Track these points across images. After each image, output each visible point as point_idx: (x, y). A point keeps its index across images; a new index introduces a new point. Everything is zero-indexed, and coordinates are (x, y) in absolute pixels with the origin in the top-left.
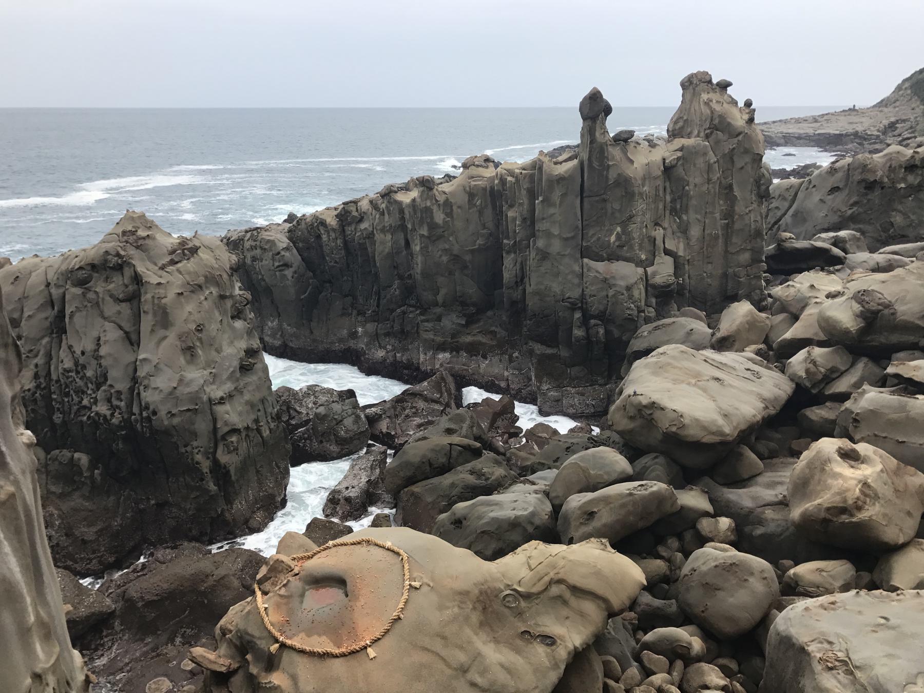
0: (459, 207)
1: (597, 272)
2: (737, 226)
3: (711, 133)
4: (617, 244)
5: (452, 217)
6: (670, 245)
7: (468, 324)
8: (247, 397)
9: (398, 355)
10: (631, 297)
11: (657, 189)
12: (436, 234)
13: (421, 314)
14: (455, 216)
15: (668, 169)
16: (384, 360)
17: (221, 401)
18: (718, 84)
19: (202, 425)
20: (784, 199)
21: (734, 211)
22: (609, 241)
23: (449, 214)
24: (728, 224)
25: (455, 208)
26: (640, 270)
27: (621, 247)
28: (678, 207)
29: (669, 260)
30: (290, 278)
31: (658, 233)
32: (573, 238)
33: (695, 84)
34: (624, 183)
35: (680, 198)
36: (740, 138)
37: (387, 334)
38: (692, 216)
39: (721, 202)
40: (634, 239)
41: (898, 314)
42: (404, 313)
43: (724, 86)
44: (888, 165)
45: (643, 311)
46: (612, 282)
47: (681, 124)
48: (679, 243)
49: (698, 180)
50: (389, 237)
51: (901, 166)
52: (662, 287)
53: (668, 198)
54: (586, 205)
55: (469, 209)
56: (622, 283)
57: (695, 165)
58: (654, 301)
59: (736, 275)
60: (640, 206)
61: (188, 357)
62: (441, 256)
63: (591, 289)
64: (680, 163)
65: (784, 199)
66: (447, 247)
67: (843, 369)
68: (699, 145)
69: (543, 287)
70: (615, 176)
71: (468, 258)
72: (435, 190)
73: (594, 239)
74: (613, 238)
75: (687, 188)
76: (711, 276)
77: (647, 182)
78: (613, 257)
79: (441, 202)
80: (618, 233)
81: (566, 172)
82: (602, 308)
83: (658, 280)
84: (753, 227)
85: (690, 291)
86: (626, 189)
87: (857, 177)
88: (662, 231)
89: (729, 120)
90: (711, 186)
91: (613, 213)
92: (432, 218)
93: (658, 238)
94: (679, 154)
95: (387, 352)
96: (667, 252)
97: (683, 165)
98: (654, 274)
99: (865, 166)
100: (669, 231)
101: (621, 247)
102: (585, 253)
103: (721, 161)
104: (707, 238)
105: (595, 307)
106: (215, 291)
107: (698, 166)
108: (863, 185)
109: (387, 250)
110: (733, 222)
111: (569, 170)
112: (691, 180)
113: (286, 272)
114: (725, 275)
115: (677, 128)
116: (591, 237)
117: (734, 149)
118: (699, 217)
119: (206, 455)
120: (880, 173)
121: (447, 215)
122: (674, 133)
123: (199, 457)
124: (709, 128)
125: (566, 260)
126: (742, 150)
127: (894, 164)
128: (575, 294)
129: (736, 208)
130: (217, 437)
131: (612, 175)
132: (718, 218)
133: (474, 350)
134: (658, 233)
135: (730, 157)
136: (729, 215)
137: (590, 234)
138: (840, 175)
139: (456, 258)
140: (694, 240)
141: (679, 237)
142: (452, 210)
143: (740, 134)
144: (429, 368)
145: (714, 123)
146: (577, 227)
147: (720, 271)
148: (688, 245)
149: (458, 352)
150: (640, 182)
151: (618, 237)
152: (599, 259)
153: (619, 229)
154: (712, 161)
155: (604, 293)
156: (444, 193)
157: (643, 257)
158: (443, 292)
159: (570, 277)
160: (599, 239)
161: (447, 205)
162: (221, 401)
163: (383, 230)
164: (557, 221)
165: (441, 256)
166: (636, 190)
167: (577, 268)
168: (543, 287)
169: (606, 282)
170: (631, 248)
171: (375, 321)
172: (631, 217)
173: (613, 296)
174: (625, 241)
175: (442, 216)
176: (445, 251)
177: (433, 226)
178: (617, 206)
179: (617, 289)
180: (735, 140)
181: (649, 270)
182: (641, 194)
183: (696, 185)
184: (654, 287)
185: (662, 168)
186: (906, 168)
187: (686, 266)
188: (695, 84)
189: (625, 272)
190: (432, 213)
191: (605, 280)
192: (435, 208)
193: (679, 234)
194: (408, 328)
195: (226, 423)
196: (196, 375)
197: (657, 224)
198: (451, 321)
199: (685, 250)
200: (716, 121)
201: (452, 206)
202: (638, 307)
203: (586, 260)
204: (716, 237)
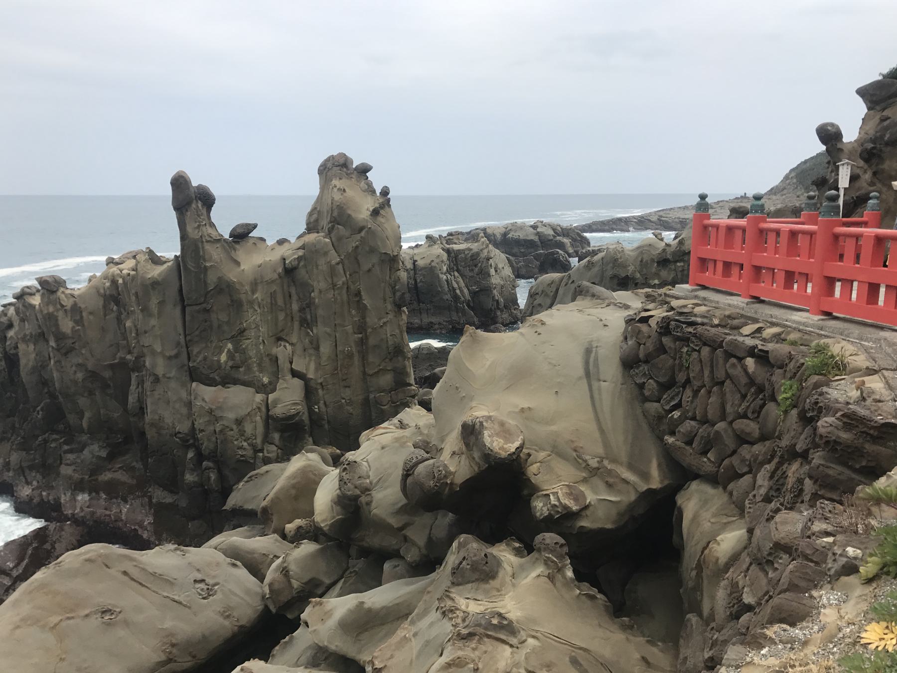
0: (91, 313)
1: (203, 400)
2: (372, 341)
3: (333, 227)
4: (230, 363)
5: (83, 325)
6: (298, 366)
7: (112, 457)
9: (44, 494)
10: (242, 433)
11: (273, 295)
12: (66, 347)
13: (65, 443)
14: (86, 324)
15: (289, 271)
16: (31, 499)
18: (356, 169)
20: (547, 295)
21: (365, 323)
22: (219, 361)
23: (79, 322)
24: (362, 339)
25: (84, 314)
26: (259, 397)
27: (236, 367)
28: (309, 317)
29: (297, 383)
31: (282, 351)
32: (176, 356)
33: (336, 168)
34: (226, 288)
35: (308, 306)
36: (363, 234)
37: (31, 468)
38: (320, 330)
39: (353, 312)
40: (250, 358)
41: (374, 505)
42: (46, 441)
43: (364, 170)
44: (640, 259)
45: (261, 451)
46: (218, 413)
47: (315, 216)
48: (310, 360)
49: (323, 285)
50: (32, 347)
51: (653, 260)
52: (283, 419)
53: (295, 307)
54: (188, 318)
55: (105, 315)
56: (231, 416)
57: (317, 266)
58: (276, 436)
59: (377, 402)
60: (252, 317)
62: (75, 372)
63: (200, 423)
64: (302, 264)
65: (547, 295)
66: (80, 361)
67: (327, 581)
68: (319, 242)
69: (157, 417)
70: (215, 280)
71: (107, 374)
72: (59, 293)
73: (200, 358)
74: (223, 358)
75: (312, 294)
76: (350, 403)
77: (260, 287)
78: (227, 381)
79: (68, 308)
80: (229, 350)
81: (159, 275)
82: (212, 446)
83: (279, 411)
84: (390, 343)
85: (329, 422)
86: (231, 296)
87: (610, 273)
88: (289, 347)
89: (349, 212)
90: (336, 292)
91: (219, 326)
92: (57, 325)
93: (280, 357)
94: (301, 253)
95: (33, 490)
96: (295, 374)
97: (305, 266)
98: (276, 402)
99: (616, 260)
100: (299, 348)
101: (236, 367)
102: (194, 375)
103: (346, 262)
104: (340, 356)
105: (207, 447)
107: (320, 267)
108: (616, 281)
109: (31, 364)
110: (367, 338)
111: (162, 272)
112: (315, 284)
114: (366, 401)
115: (312, 220)
116: (197, 356)
117: (357, 247)
118: (328, 330)
120: (631, 268)
121: (77, 322)
122: (312, 227)
124: (331, 222)
125: (173, 384)
126: (367, 249)
127: (646, 258)
128: (183, 427)
129: (368, 319)
131: (212, 278)
132: (351, 331)
133: (113, 491)
134: (282, 351)
135: (354, 257)
136: (361, 328)
137: (195, 353)
138: (596, 269)
139: (93, 375)
140: (324, 359)
141: (310, 355)
142: (82, 317)
143: (361, 229)
144: (70, 512)
145: (348, 215)
146: (178, 344)
147: (361, 397)
148: (319, 366)
149: (97, 493)
150: (247, 288)
151: (231, 356)
152: (211, 383)
153: (230, 346)
154: (333, 262)
155: (212, 428)
156: (73, 296)
157: (266, 380)
158: (87, 415)
159: (177, 406)
160: (205, 358)
161: (76, 311)
163: (24, 339)
164: (157, 336)
165: (75, 372)
166: (243, 297)
167: (184, 394)
168: (157, 417)
169: (213, 415)
170: (249, 369)
171: (24, 450)
172: (242, 331)
173: (221, 431)
174: (240, 361)
175: (71, 324)
176: (79, 365)
177: (60, 337)
178: (223, 317)
179: (225, 423)
180: (358, 237)
181: (271, 397)
182: (251, 303)
183: (320, 292)
184: (276, 419)
185: (280, 270)
186: (658, 263)
187: (320, 391)
188: (336, 168)
189: (238, 400)
190: (57, 320)
191: (211, 412)
192: (60, 314)
193: (312, 351)
194: (50, 461)
197: (279, 339)
198: (95, 450)
199: (317, 369)
200: (335, 214)
201: (81, 312)
202: (253, 446)
203: (194, 384)
204: (350, 356)
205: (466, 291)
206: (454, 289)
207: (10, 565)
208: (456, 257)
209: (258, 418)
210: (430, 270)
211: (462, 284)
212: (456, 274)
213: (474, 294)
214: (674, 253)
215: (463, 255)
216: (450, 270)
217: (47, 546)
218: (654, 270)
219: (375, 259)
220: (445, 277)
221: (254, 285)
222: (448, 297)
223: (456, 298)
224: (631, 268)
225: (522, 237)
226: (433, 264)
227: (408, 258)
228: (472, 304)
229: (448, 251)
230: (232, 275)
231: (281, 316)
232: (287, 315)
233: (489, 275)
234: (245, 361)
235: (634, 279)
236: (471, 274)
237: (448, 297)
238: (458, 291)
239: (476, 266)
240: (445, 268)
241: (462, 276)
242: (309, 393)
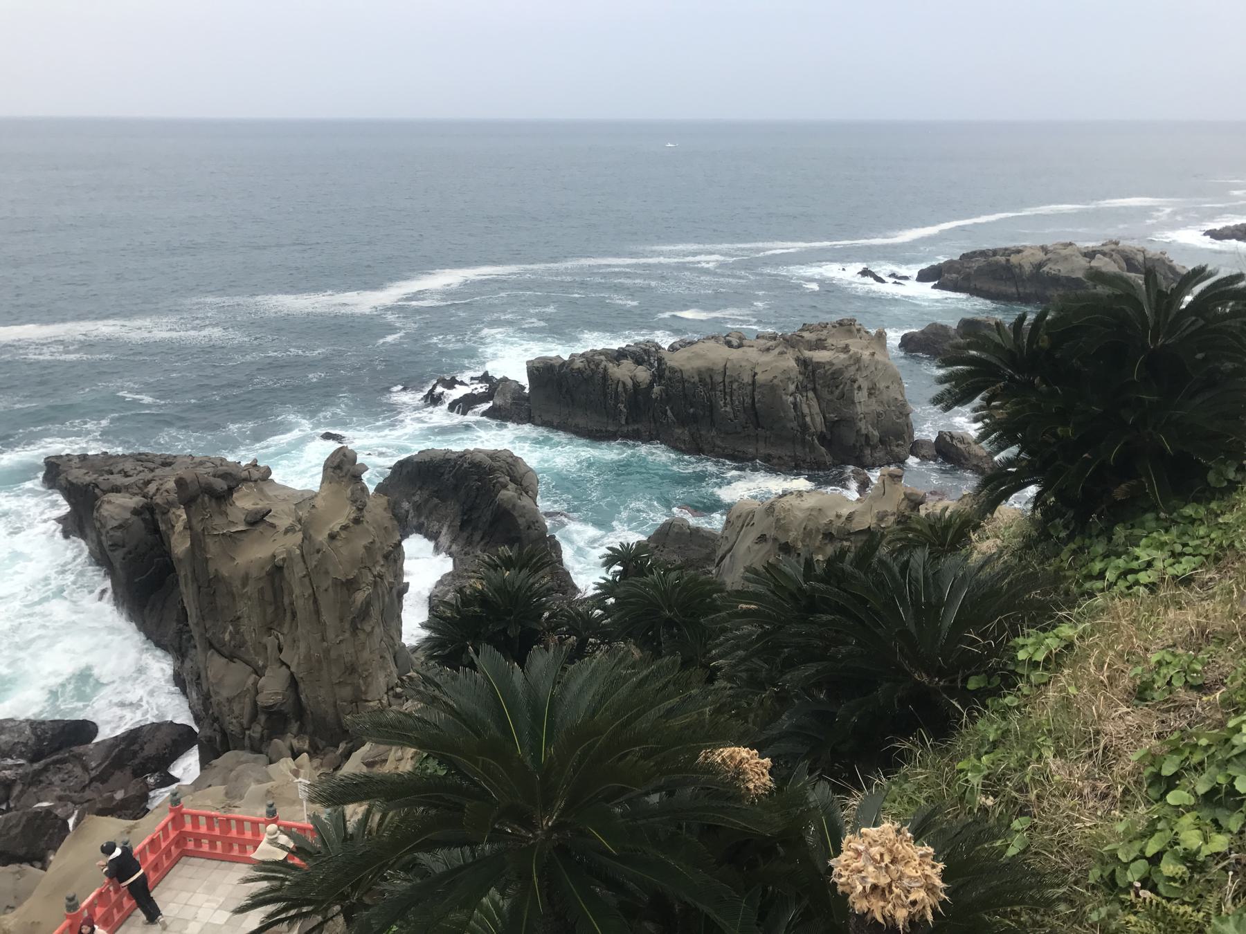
2: (333, 654)
45: (249, 729)
72: (170, 514)
113: (116, 553)
120: (793, 534)
127: (811, 525)
150: (238, 583)
151: (232, 637)
153: (231, 628)
172: (239, 618)
204: (319, 661)
205: (819, 419)
206: (804, 416)
207: (93, 764)
208: (814, 372)
209: (247, 700)
210: (772, 388)
211: (816, 409)
212: (811, 394)
213: (832, 425)
214: (839, 529)
215: (822, 371)
216: (801, 389)
217: (136, 747)
218: (818, 544)
219: (330, 582)
220: (791, 399)
221: (245, 580)
222: (794, 424)
223: (804, 427)
224: (793, 534)
225: (1064, 273)
226: (775, 381)
227: (749, 366)
228: (829, 437)
229: (804, 363)
230: (225, 572)
231: (270, 610)
232: (277, 608)
233: (853, 402)
234: (242, 644)
235: (796, 549)
236: (830, 397)
237: (794, 424)
238: (808, 419)
239: (837, 387)
240: (792, 388)
241: (818, 397)
242: (294, 683)
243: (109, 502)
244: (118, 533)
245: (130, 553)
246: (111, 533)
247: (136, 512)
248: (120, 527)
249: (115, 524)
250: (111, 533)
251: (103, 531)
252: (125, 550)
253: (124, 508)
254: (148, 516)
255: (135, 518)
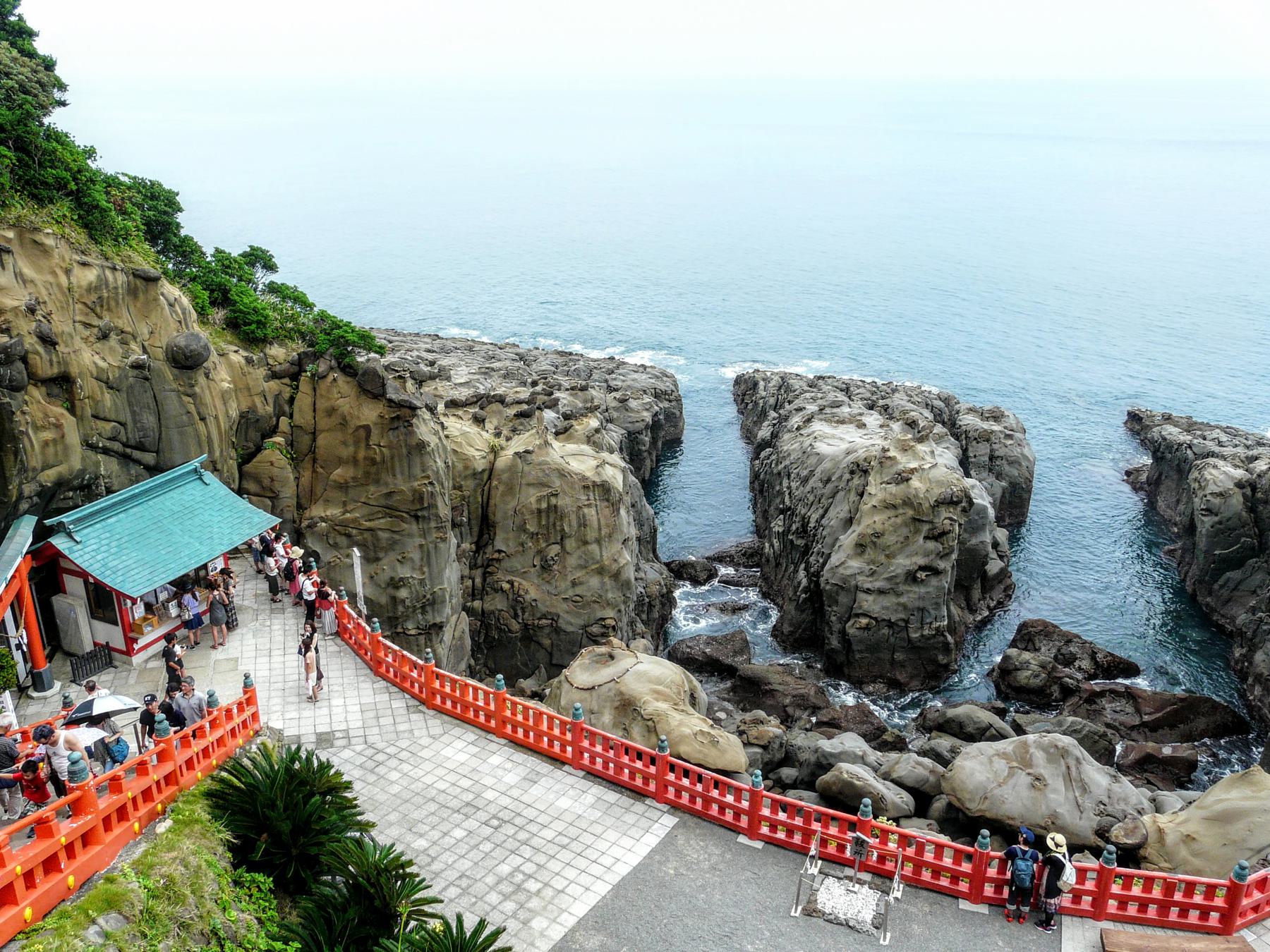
8: (903, 600)
17: (868, 591)
19: (843, 599)
30: (1207, 526)
61: (859, 551)
106: (910, 513)
119: (840, 620)
123: (833, 618)
130: (851, 614)
162: (868, 591)
195: (860, 607)
196: (855, 564)
207: (1148, 710)
243: (1215, 467)
244: (1217, 501)
245: (1220, 523)
246: (1209, 497)
247: (1240, 485)
248: (1221, 495)
249: (1217, 490)
250: (1209, 497)
251: (1200, 494)
252: (1216, 519)
253: (1232, 478)
254: (1248, 491)
255: (1237, 490)
